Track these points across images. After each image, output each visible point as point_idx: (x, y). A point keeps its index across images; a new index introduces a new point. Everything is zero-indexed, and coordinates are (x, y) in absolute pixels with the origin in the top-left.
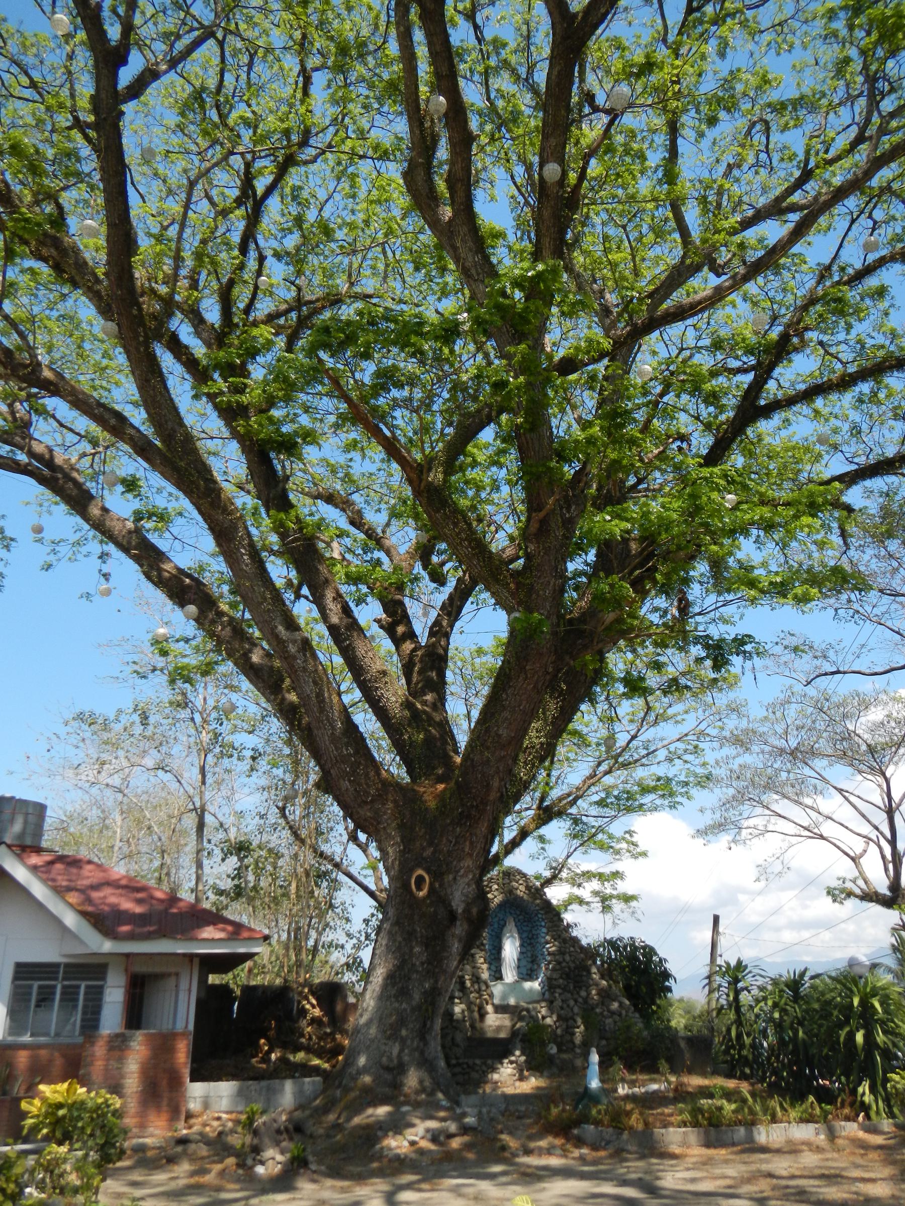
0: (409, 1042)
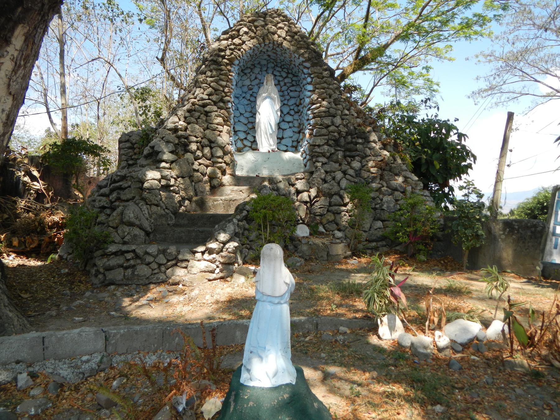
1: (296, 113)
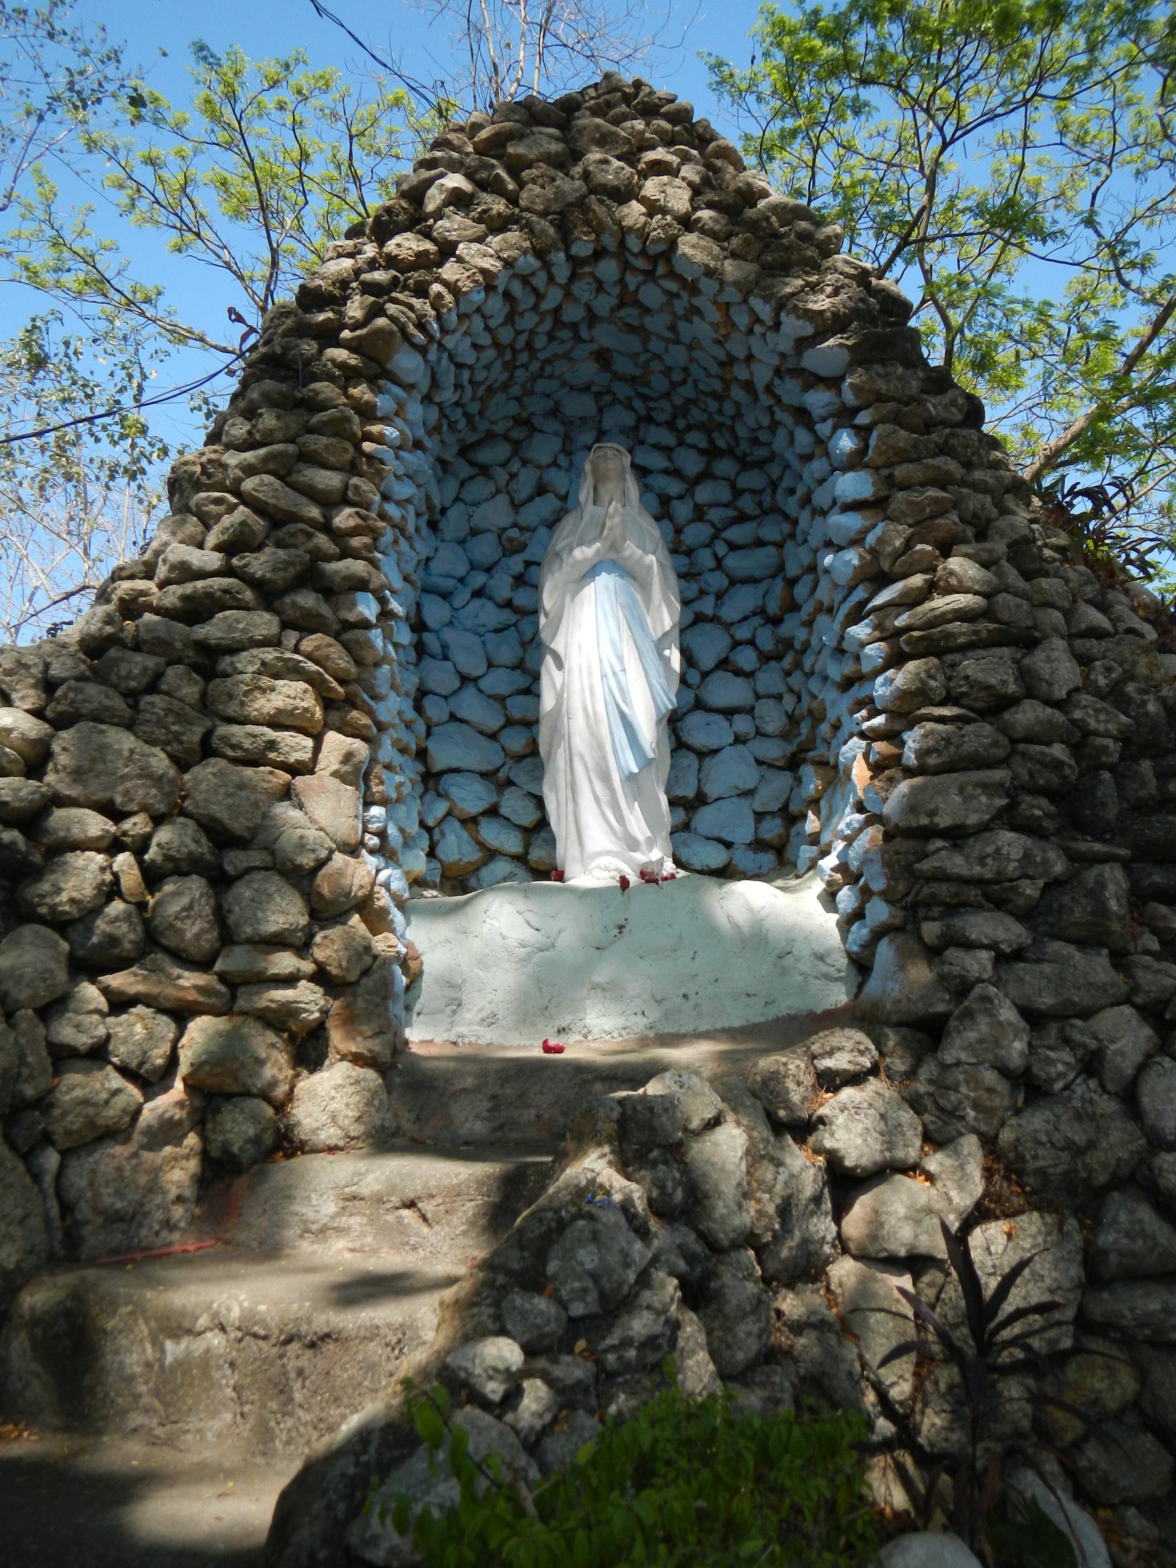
1: (766, 658)
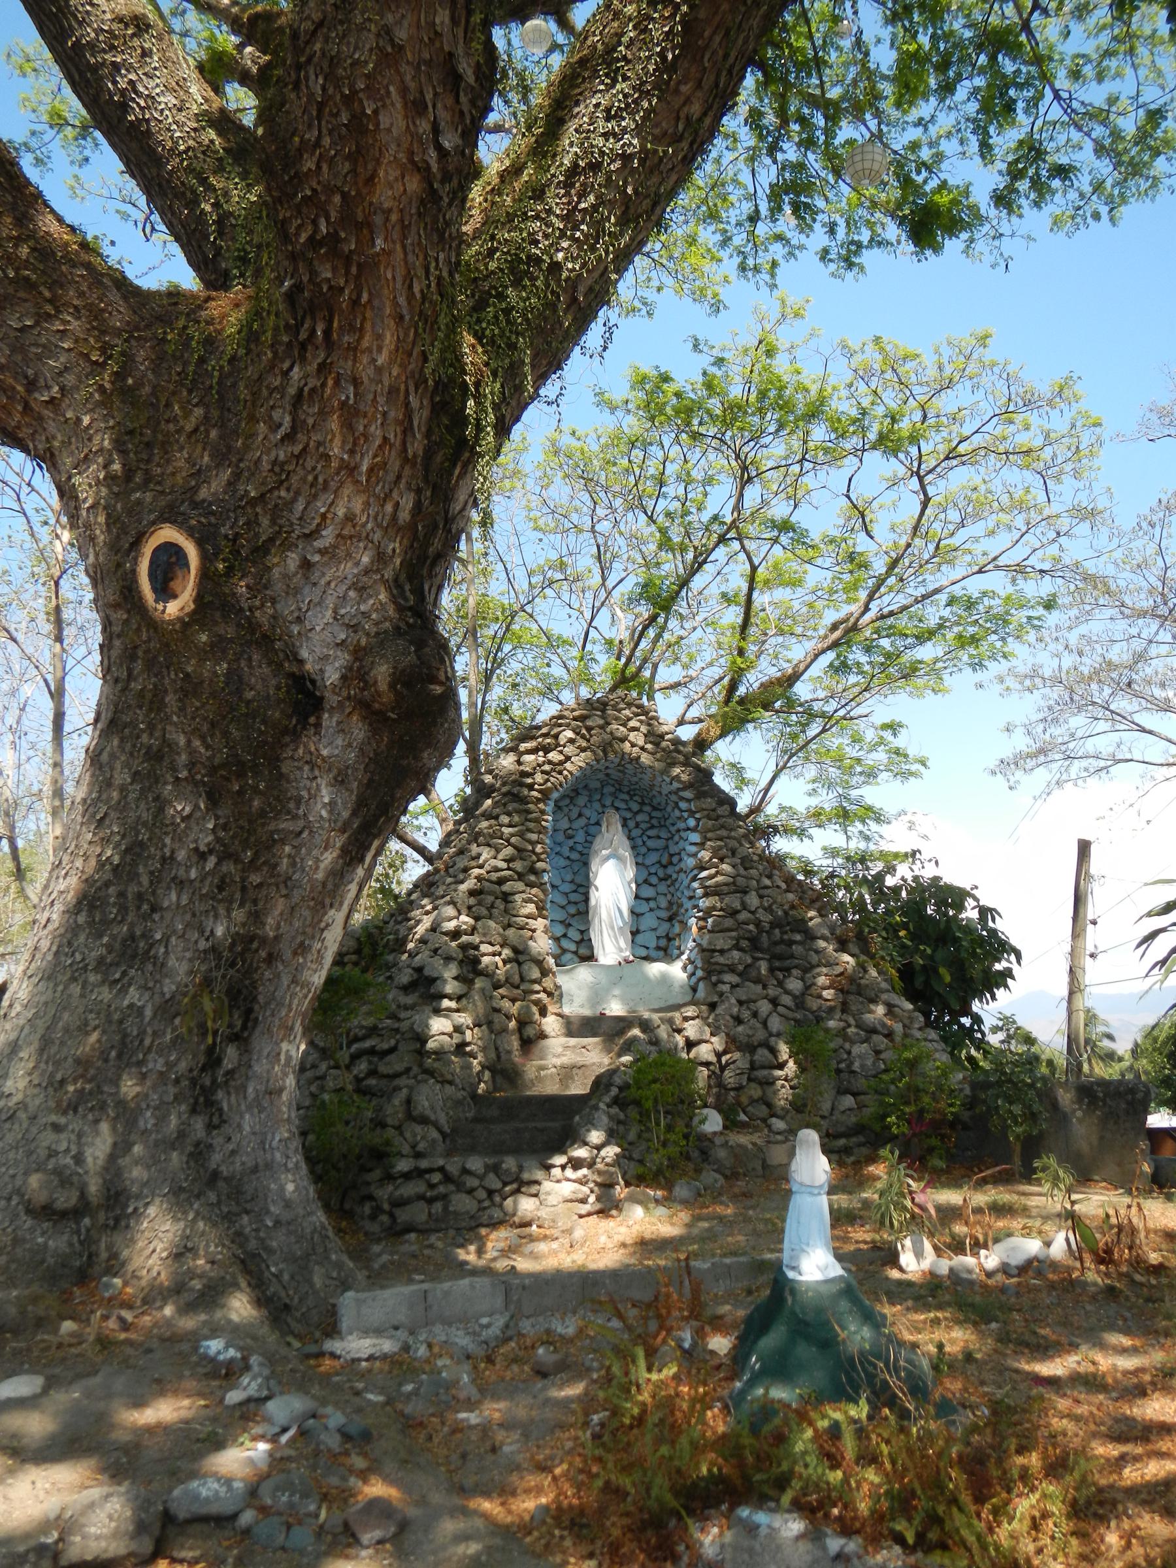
0: (148, 1120)
1: (661, 880)
